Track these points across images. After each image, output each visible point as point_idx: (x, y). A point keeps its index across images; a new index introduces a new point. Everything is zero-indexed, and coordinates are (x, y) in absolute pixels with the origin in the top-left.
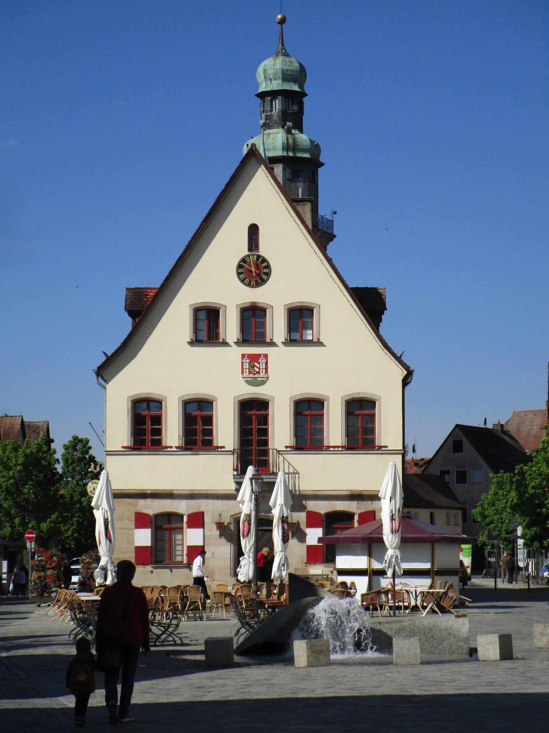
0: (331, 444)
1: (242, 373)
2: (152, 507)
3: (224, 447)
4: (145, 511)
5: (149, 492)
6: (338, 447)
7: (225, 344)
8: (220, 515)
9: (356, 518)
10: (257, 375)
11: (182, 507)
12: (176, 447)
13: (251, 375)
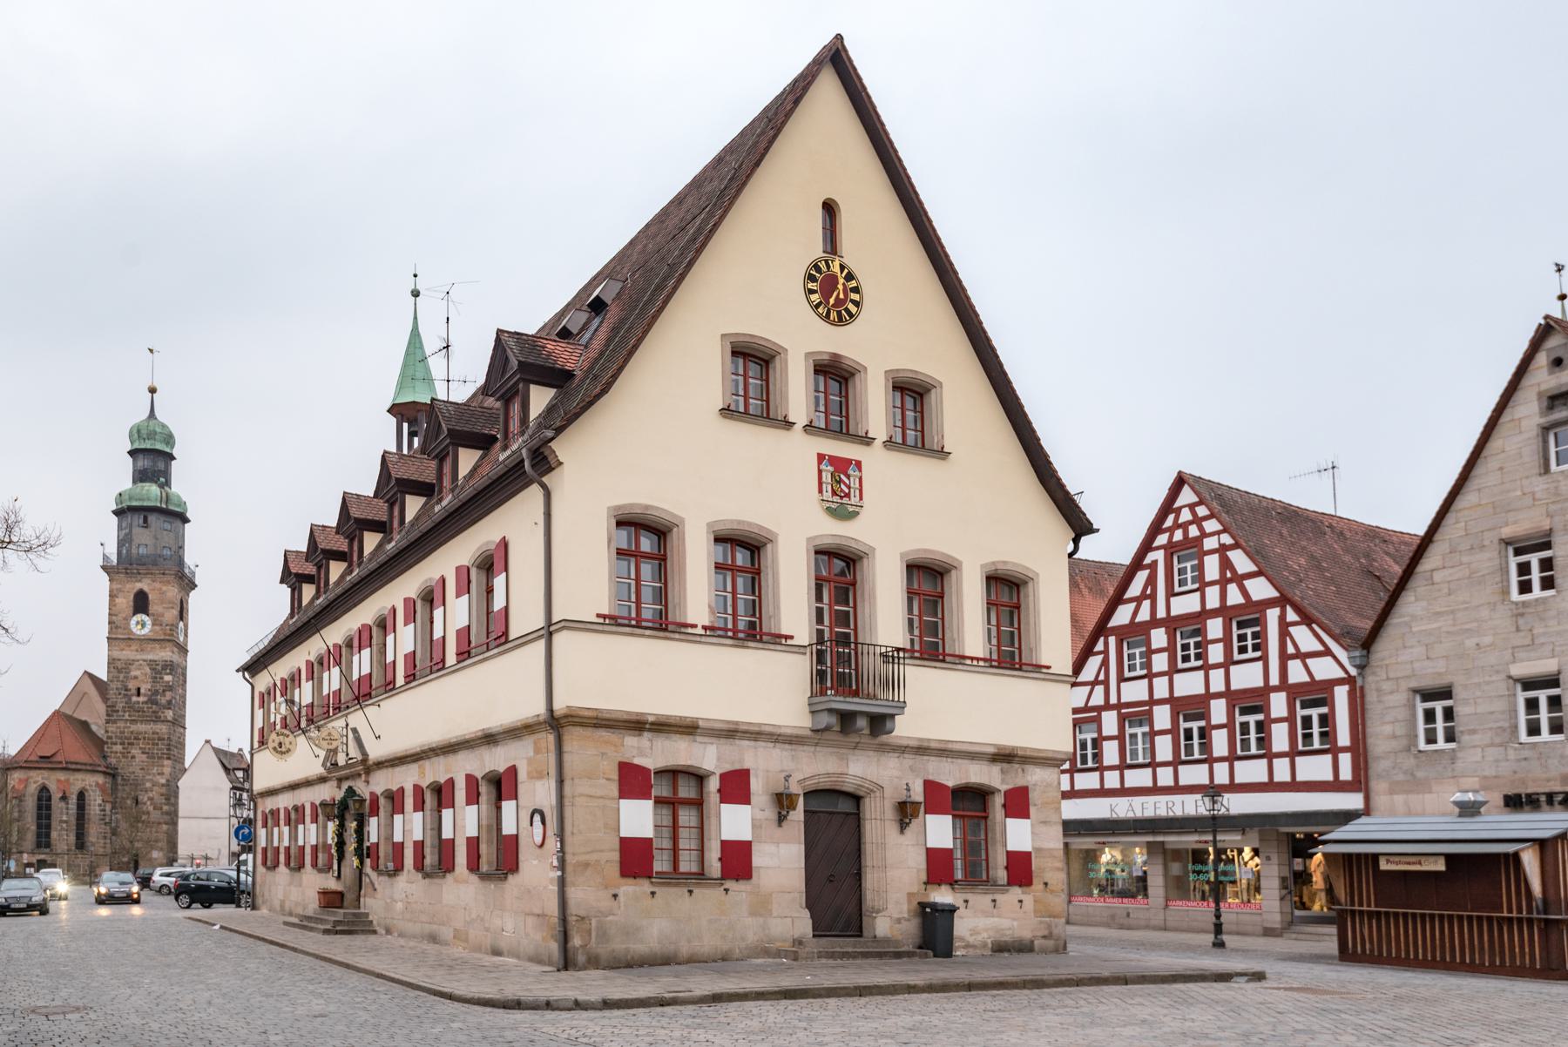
0: (967, 654)
1: (820, 491)
2: (654, 754)
3: (792, 637)
4: (637, 761)
5: (651, 719)
6: (978, 659)
7: (788, 425)
8: (787, 778)
9: (999, 800)
10: (845, 500)
11: (710, 758)
12: (705, 628)
13: (836, 499)
